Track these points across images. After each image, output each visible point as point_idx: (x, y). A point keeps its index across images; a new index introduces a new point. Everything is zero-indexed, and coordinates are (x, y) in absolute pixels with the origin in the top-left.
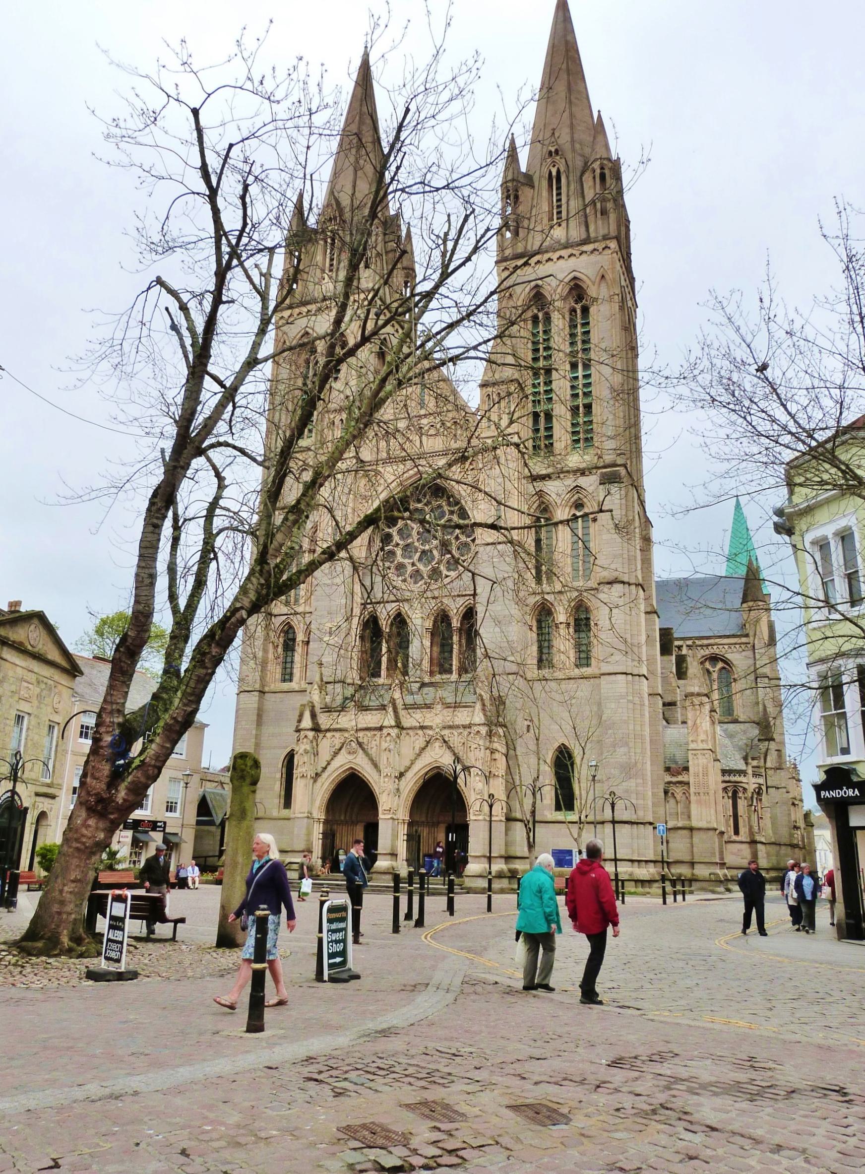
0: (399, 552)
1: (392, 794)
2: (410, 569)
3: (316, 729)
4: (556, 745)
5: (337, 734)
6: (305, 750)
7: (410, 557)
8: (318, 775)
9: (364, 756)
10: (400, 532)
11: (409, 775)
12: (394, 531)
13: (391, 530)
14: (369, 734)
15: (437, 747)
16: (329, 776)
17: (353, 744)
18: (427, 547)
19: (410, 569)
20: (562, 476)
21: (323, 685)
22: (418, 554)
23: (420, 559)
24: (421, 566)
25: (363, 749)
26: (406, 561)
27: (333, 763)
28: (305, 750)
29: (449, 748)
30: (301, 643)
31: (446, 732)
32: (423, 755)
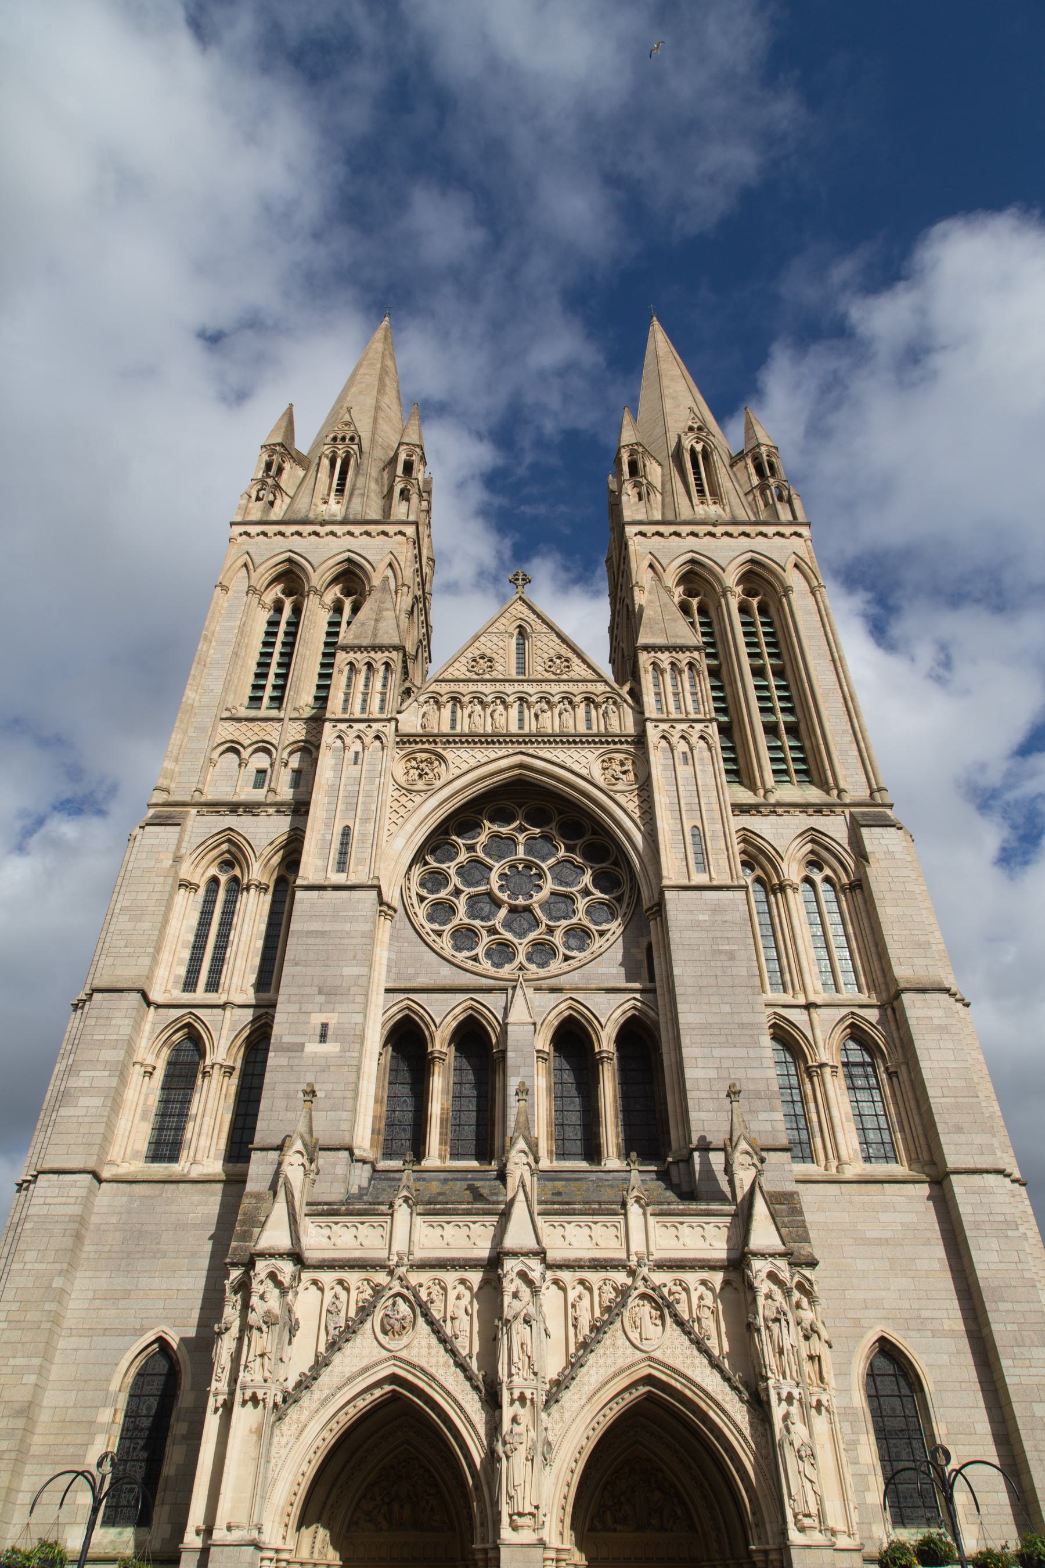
0: (461, 904)
1: (539, 1459)
2: (485, 939)
3: (297, 1257)
4: (872, 1336)
5: (353, 1278)
6: (268, 1313)
7: (482, 919)
8: (289, 1399)
9: (434, 1340)
10: (461, 871)
11: (570, 1398)
12: (451, 868)
13: (444, 866)
14: (450, 1277)
15: (647, 1321)
16: (324, 1402)
17: (403, 1308)
18: (521, 901)
19: (485, 939)
20: (780, 810)
21: (313, 1151)
22: (503, 912)
23: (507, 925)
24: (509, 936)
25: (431, 1322)
26: (477, 923)
27: (337, 1358)
28: (268, 1313)
29: (680, 1323)
30: (216, 1073)
31: (658, 1278)
32: (607, 1340)
